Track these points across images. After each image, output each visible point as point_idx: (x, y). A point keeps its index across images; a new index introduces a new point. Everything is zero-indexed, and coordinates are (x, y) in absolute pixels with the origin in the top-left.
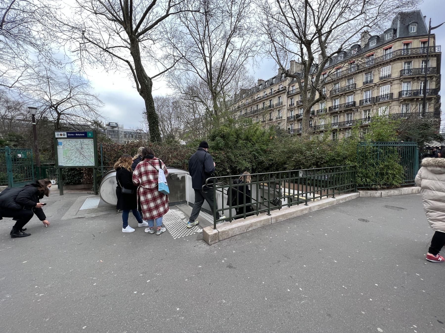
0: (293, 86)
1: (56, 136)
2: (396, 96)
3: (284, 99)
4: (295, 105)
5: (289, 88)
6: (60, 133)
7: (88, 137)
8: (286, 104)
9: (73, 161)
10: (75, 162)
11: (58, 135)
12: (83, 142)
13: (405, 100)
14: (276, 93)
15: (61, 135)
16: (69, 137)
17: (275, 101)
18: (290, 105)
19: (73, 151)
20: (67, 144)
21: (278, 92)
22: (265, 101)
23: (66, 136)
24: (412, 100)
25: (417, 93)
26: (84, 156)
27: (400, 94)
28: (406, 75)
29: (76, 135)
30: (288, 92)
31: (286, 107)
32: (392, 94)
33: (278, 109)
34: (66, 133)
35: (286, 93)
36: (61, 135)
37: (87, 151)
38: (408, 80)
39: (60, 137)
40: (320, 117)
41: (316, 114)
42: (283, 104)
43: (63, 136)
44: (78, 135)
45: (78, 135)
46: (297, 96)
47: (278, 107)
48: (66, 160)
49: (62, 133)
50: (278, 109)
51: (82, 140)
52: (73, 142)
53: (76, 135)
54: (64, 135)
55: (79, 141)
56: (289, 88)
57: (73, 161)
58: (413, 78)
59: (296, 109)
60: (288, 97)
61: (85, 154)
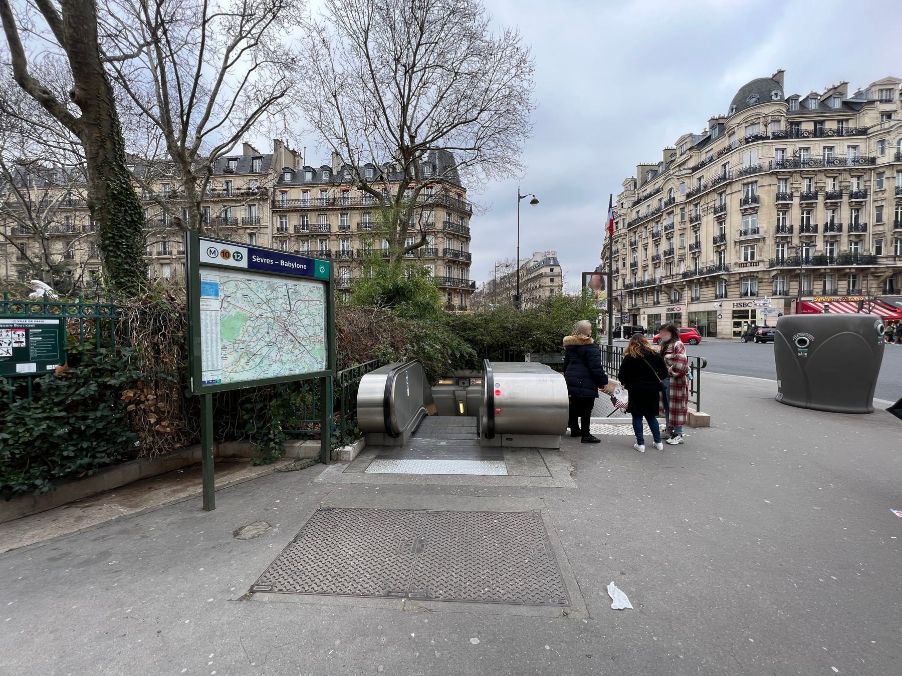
0: (283, 193)
1: (204, 258)
2: (441, 254)
3: (264, 213)
4: (291, 231)
5: (274, 192)
6: (220, 247)
7: (316, 275)
8: (269, 224)
9: (258, 360)
10: (266, 362)
11: (210, 252)
12: (296, 292)
13: (449, 261)
14: (242, 194)
15: (225, 254)
16: (254, 268)
17: (239, 213)
18: (278, 229)
19: (260, 322)
20: (239, 295)
21: (248, 194)
22: (211, 205)
23: (244, 264)
24: (454, 262)
25: (456, 254)
26: (296, 339)
27: (445, 251)
28: (449, 230)
29: (282, 263)
30: (273, 202)
31: (269, 230)
32: (437, 250)
33: (249, 231)
34: (244, 252)
35: (269, 201)
36: (225, 254)
37: (306, 322)
38: (451, 236)
39: (220, 261)
40: (342, 265)
41: (334, 257)
42: (262, 224)
43: (231, 262)
44: (288, 264)
45: (288, 264)
46: (294, 214)
47: (249, 226)
48: (231, 358)
49: (232, 249)
50: (249, 231)
51: (290, 283)
52: (261, 285)
53: (282, 263)
54: (238, 256)
55: (282, 285)
56: (274, 192)
57: (258, 360)
58: (453, 235)
59: (293, 239)
60: (273, 212)
61: (300, 334)
